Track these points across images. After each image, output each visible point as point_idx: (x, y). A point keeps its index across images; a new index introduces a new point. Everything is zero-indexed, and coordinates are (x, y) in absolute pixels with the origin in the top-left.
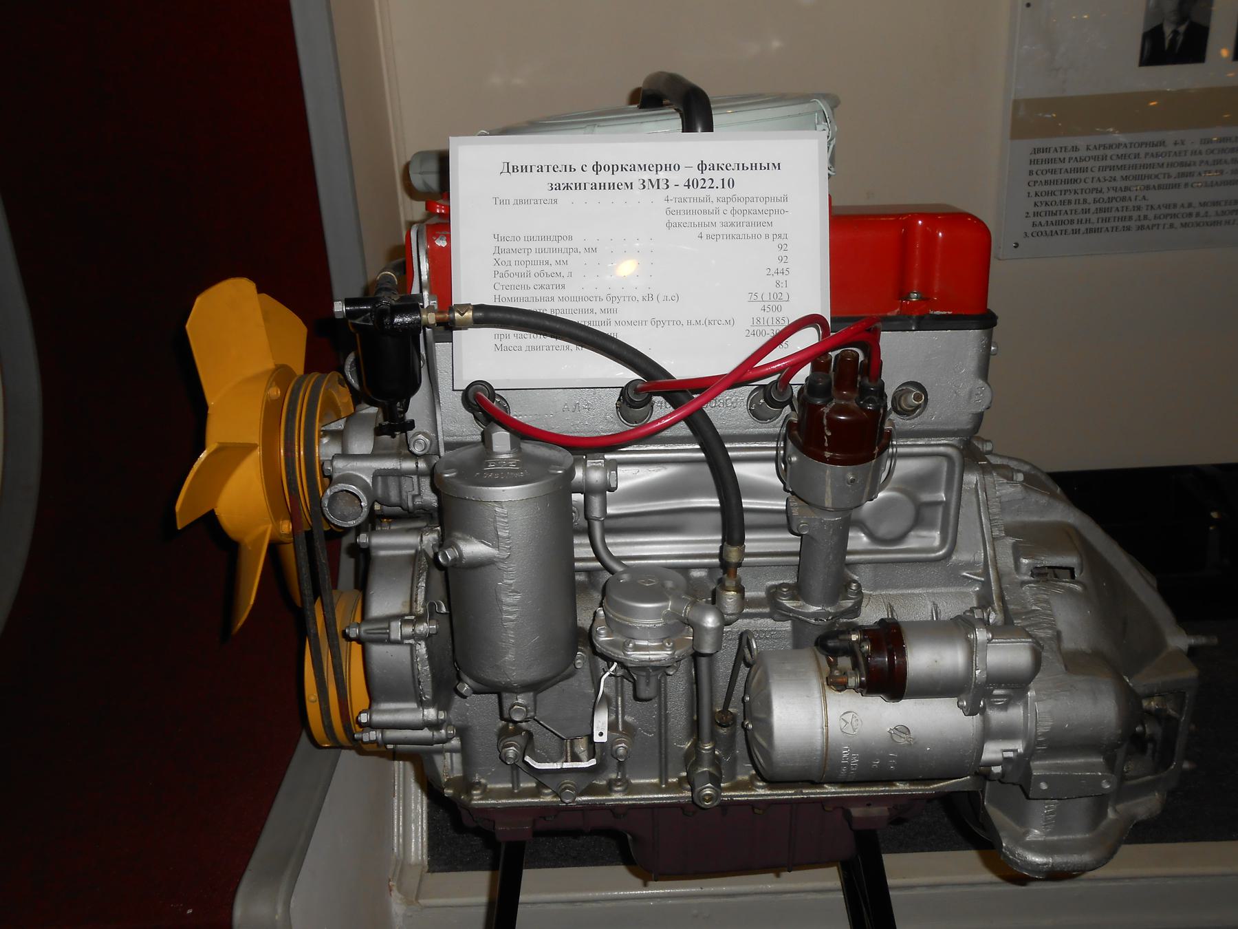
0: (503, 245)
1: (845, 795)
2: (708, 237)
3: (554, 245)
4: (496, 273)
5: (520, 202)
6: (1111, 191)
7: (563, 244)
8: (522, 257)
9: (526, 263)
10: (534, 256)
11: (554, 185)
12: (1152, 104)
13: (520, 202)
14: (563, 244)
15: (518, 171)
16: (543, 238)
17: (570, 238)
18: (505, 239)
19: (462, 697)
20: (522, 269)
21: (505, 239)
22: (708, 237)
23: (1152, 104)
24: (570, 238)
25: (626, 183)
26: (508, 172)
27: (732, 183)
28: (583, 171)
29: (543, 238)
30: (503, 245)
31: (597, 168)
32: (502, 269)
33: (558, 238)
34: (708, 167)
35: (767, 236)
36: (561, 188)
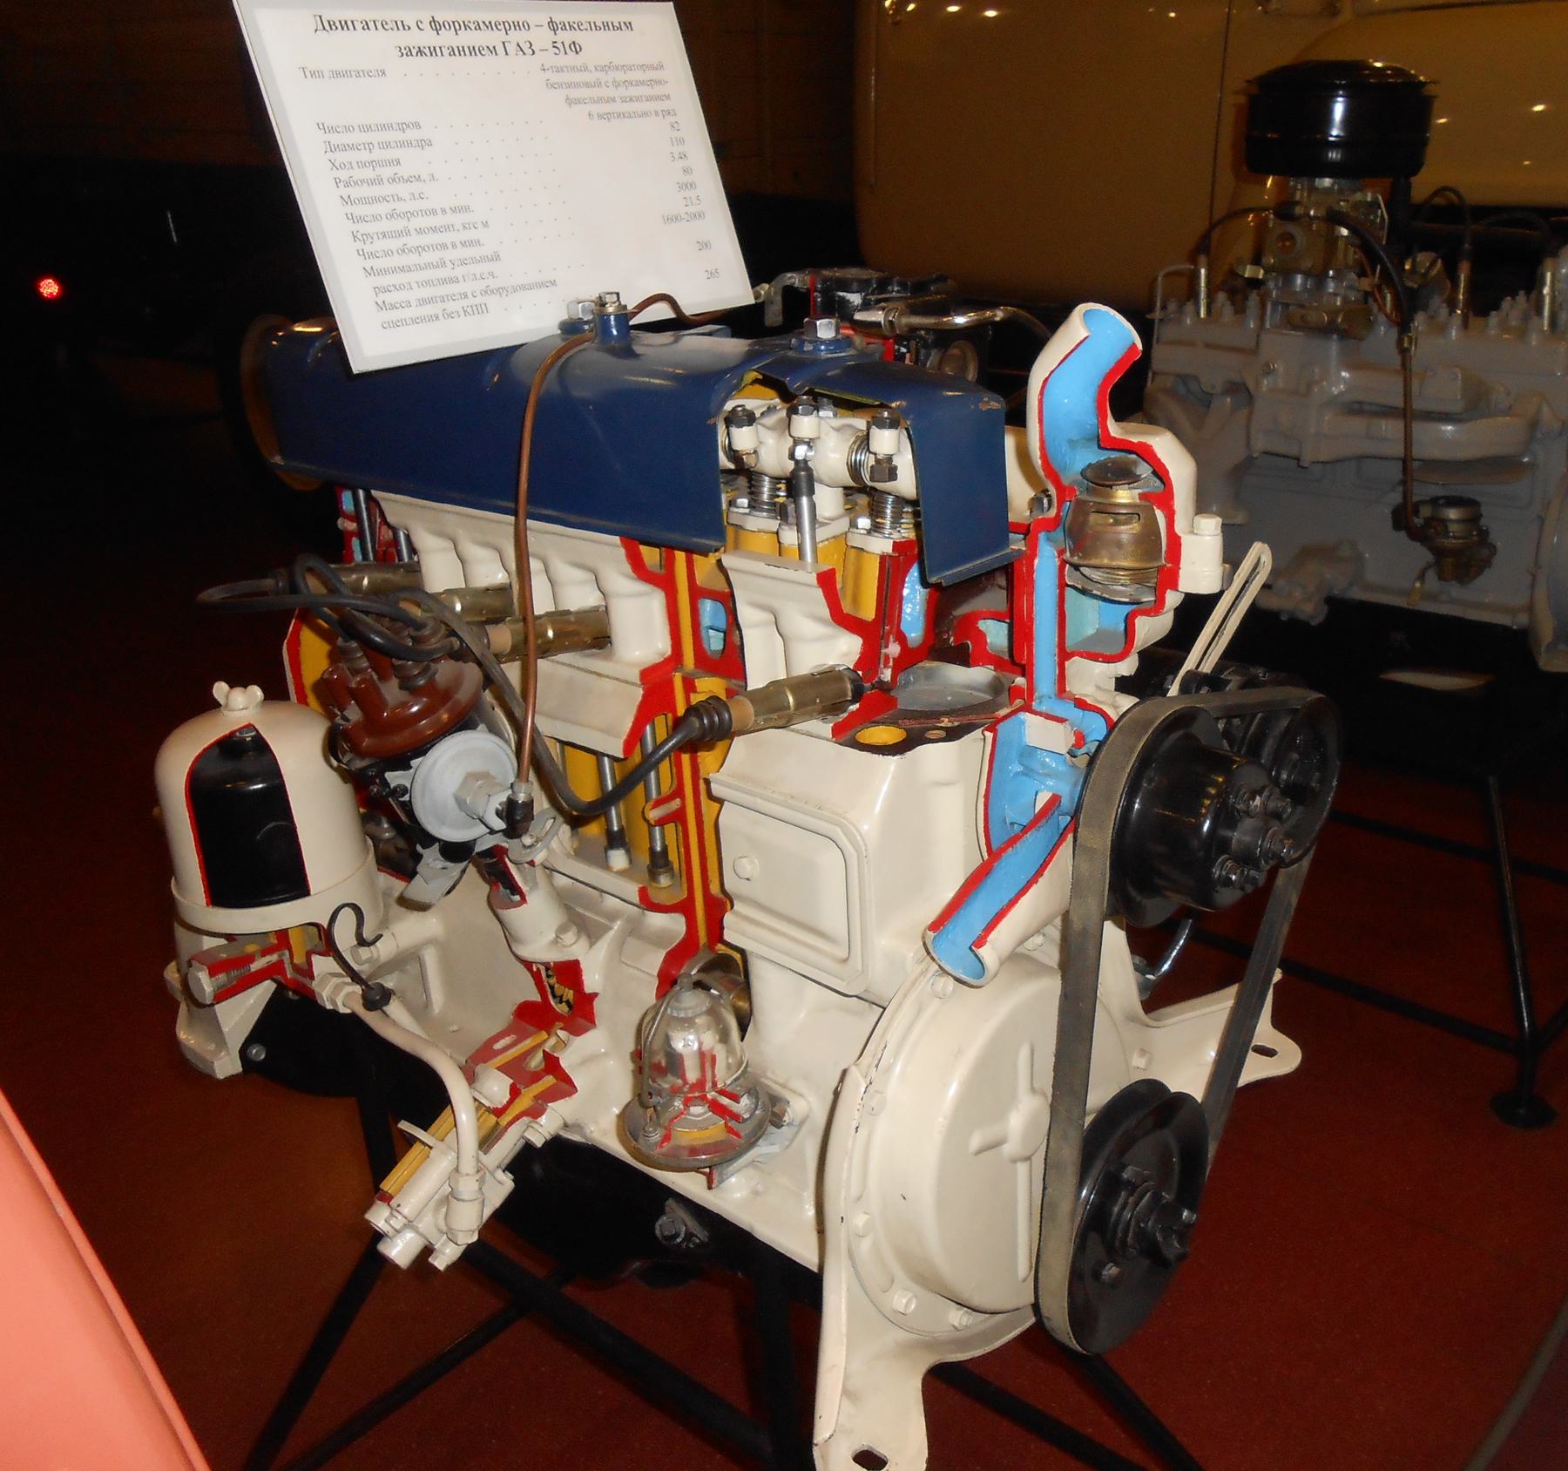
0: (335, 139)
1: (859, 838)
2: (601, 117)
3: (399, 136)
4: (338, 181)
5: (337, 74)
6: (411, 22)
7: (412, 135)
8: (364, 156)
9: (372, 164)
10: (378, 154)
11: (403, 49)
12: (1339, 109)
13: (337, 74)
14: (412, 135)
15: (337, 28)
16: (384, 127)
17: (417, 125)
18: (333, 130)
19: (360, 909)
20: (368, 173)
21: (333, 130)
22: (601, 117)
23: (1339, 109)
24: (417, 125)
25: (488, 47)
26: (324, 29)
27: (576, 48)
28: (421, 29)
29: (384, 127)
30: (335, 139)
31: (436, 26)
32: (343, 175)
33: (403, 127)
34: (560, 26)
35: (657, 113)
36: (414, 54)
